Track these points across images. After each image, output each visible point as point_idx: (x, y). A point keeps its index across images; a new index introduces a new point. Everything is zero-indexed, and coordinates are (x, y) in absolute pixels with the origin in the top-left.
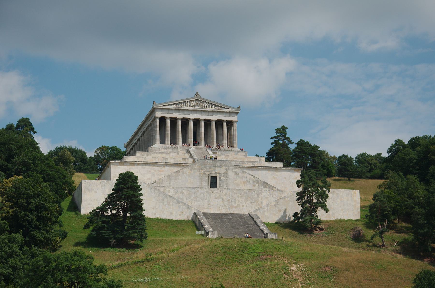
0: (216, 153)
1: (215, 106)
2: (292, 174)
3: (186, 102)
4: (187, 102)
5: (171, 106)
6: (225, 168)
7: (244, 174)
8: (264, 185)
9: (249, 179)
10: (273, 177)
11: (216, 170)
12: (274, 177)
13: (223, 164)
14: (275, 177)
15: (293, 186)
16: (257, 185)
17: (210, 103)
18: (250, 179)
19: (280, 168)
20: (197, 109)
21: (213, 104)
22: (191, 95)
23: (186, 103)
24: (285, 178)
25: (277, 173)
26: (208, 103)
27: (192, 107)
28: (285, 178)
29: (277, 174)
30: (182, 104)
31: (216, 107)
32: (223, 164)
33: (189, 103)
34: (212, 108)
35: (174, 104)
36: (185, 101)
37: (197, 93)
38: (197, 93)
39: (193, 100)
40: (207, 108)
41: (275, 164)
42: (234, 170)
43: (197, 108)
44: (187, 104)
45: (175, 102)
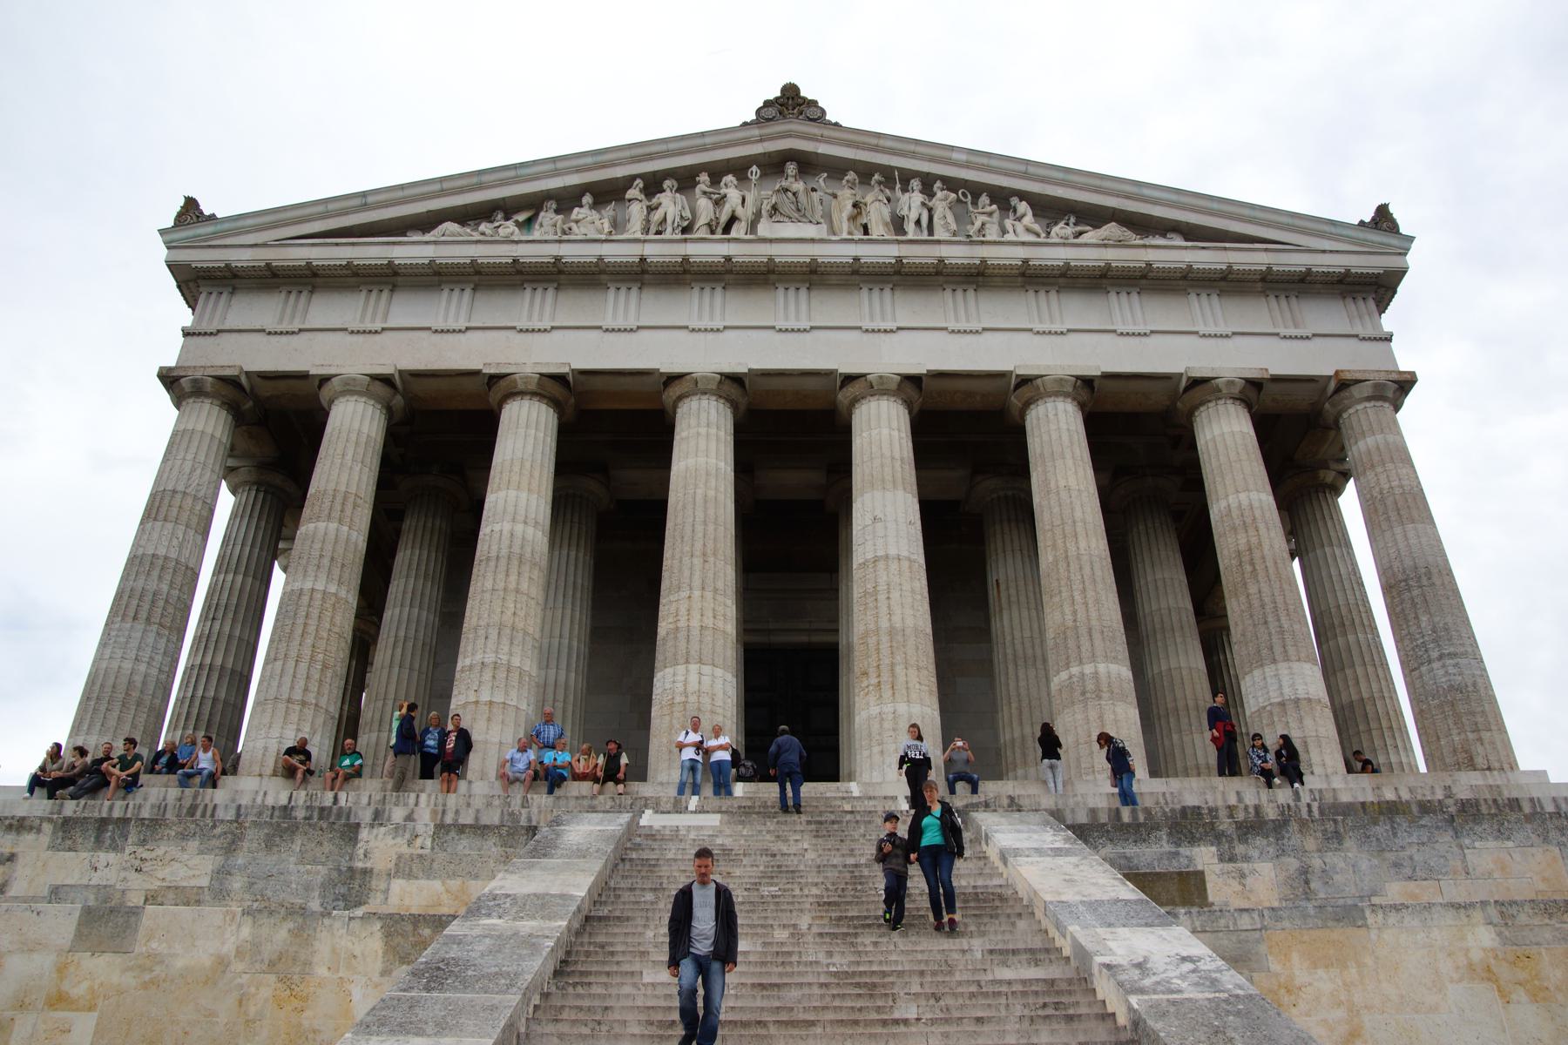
1: (1050, 210)
3: (629, 181)
4: (653, 185)
5: (427, 237)
17: (976, 190)
21: (1023, 196)
23: (631, 193)
26: (951, 184)
27: (727, 229)
30: (577, 213)
31: (1061, 230)
33: (670, 204)
36: (619, 172)
39: (739, 169)
40: (940, 234)
44: (636, 211)
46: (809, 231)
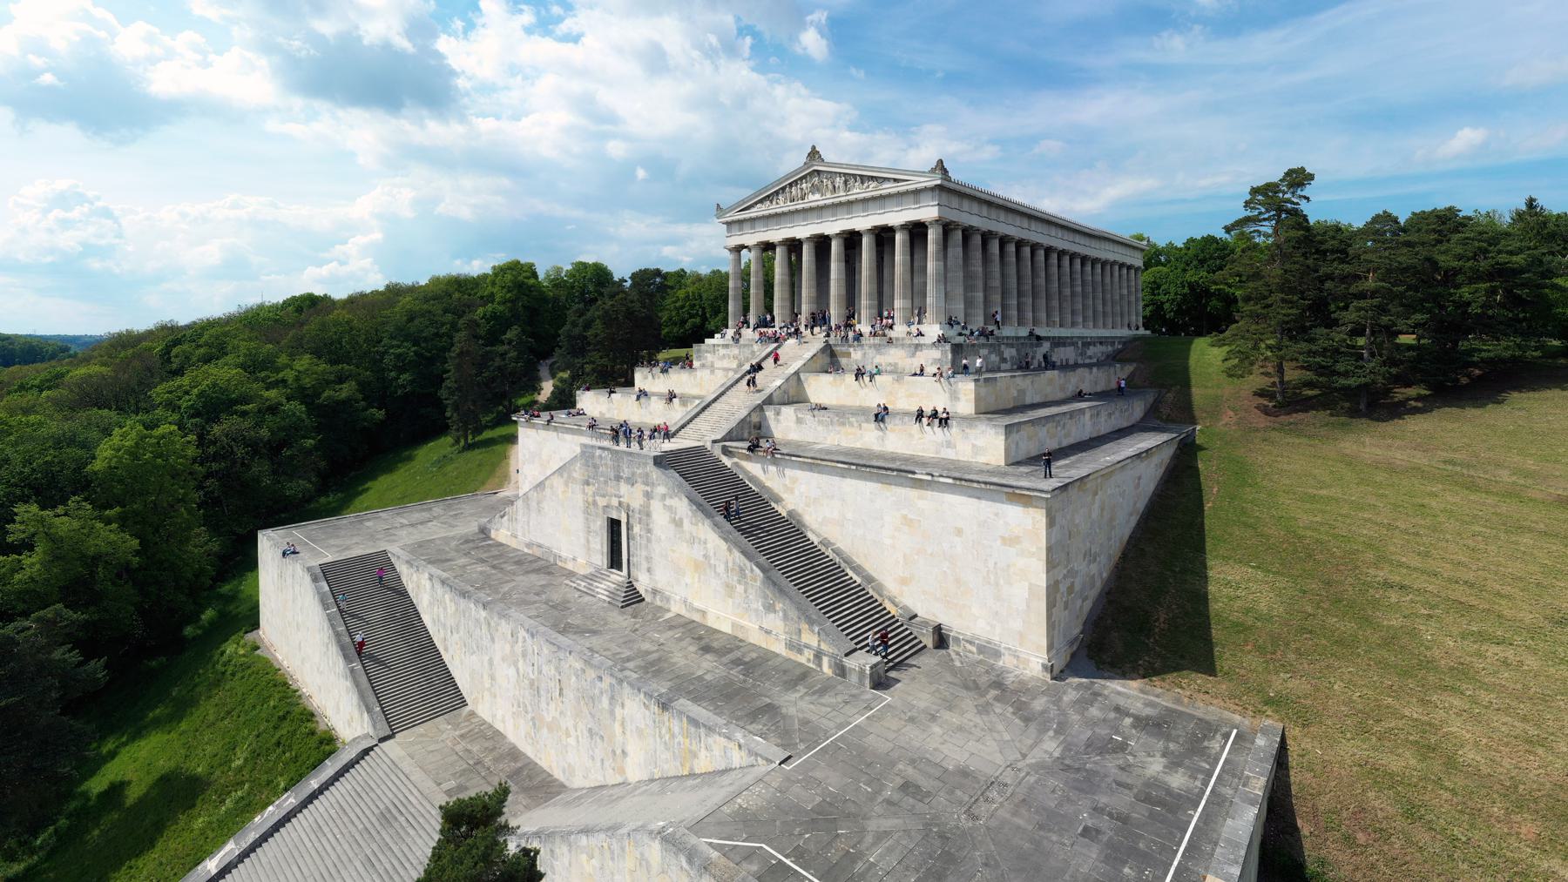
0: (849, 355)
2: (997, 515)
4: (791, 185)
6: (643, 486)
7: (697, 525)
8: (765, 597)
9: (712, 554)
10: (905, 517)
11: (622, 494)
12: (907, 521)
13: (639, 471)
14: (911, 520)
15: (997, 584)
16: (740, 588)
18: (715, 554)
19: (929, 478)
20: (813, 204)
22: (794, 161)
24: (959, 532)
25: (920, 498)
26: (845, 174)
28: (959, 532)
29: (921, 504)
32: (639, 471)
34: (858, 192)
35: (756, 203)
37: (814, 147)
38: (814, 147)
39: (804, 177)
41: (967, 431)
42: (668, 502)
43: (815, 199)
45: (761, 194)
46: (817, 196)
